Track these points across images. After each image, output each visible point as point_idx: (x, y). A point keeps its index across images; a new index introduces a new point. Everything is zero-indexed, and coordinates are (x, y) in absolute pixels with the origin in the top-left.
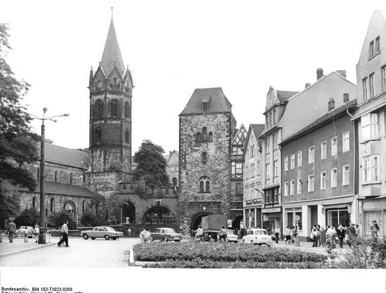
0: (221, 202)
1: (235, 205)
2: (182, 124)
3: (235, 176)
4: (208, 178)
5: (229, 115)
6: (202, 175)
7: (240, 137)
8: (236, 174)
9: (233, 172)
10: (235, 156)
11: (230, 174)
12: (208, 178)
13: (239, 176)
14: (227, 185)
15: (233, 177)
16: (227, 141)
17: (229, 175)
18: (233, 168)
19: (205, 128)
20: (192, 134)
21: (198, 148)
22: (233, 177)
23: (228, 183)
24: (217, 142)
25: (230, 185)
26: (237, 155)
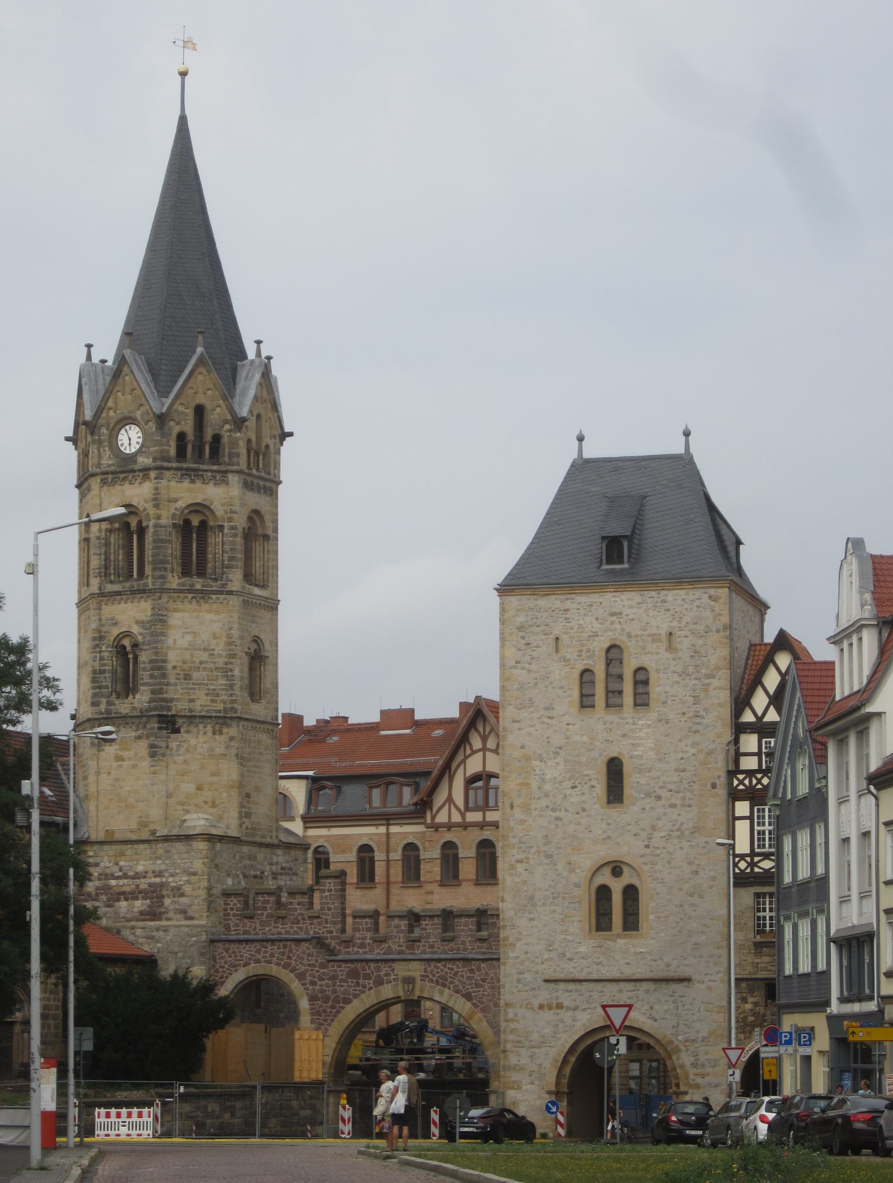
1: (751, 991)
3: (752, 865)
7: (771, 691)
8: (753, 854)
10: (750, 773)
13: (767, 864)
15: (743, 865)
18: (742, 829)
26: (759, 771)
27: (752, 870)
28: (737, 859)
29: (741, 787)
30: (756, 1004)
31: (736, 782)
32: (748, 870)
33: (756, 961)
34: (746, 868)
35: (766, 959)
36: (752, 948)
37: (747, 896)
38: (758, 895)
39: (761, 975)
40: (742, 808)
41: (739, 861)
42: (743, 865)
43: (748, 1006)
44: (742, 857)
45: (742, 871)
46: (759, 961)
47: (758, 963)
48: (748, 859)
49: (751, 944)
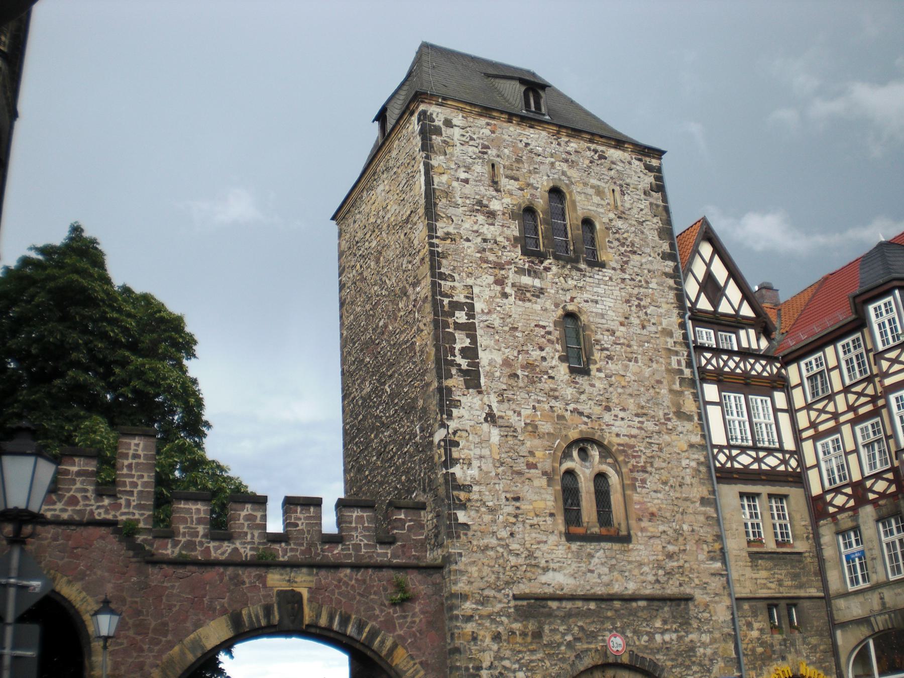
0: (688, 599)
2: (436, 139)
3: (731, 458)
4: (606, 452)
5: (655, 162)
6: (574, 435)
9: (718, 437)
11: (706, 444)
12: (606, 452)
13: (745, 460)
14: (704, 501)
16: (667, 275)
17: (703, 447)
18: (714, 413)
19: (556, 193)
20: (495, 205)
21: (537, 283)
22: (722, 458)
23: (704, 491)
24: (623, 270)
25: (710, 501)
27: (732, 464)
28: (716, 451)
29: (710, 367)
30: (761, 630)
31: (704, 362)
32: (729, 465)
33: (754, 576)
34: (726, 463)
35: (763, 574)
36: (748, 559)
37: (729, 493)
38: (742, 495)
39: (763, 593)
40: (711, 391)
41: (718, 453)
42: (722, 458)
43: (755, 634)
44: (721, 448)
45: (723, 465)
46: (757, 576)
47: (756, 579)
48: (726, 451)
49: (745, 554)
